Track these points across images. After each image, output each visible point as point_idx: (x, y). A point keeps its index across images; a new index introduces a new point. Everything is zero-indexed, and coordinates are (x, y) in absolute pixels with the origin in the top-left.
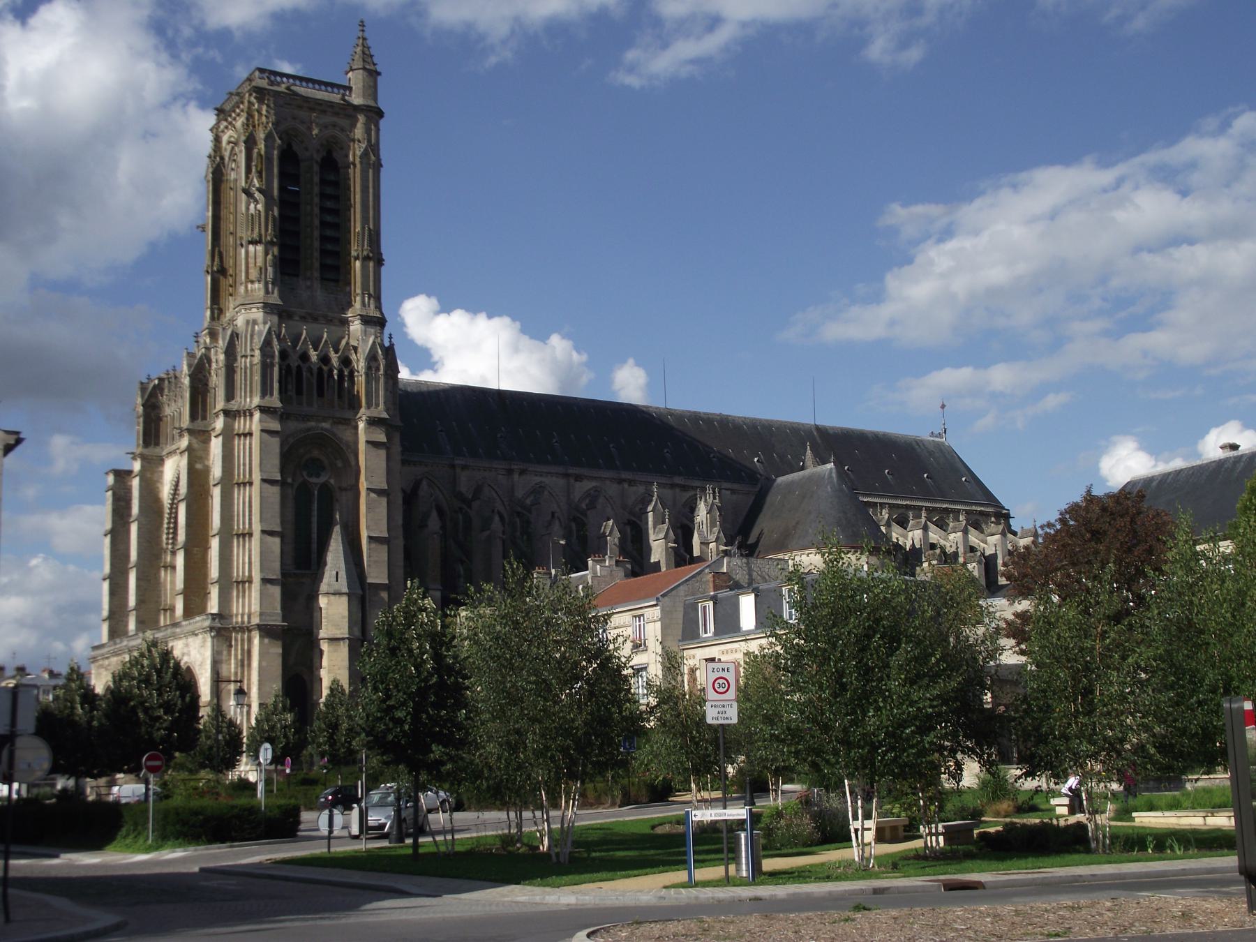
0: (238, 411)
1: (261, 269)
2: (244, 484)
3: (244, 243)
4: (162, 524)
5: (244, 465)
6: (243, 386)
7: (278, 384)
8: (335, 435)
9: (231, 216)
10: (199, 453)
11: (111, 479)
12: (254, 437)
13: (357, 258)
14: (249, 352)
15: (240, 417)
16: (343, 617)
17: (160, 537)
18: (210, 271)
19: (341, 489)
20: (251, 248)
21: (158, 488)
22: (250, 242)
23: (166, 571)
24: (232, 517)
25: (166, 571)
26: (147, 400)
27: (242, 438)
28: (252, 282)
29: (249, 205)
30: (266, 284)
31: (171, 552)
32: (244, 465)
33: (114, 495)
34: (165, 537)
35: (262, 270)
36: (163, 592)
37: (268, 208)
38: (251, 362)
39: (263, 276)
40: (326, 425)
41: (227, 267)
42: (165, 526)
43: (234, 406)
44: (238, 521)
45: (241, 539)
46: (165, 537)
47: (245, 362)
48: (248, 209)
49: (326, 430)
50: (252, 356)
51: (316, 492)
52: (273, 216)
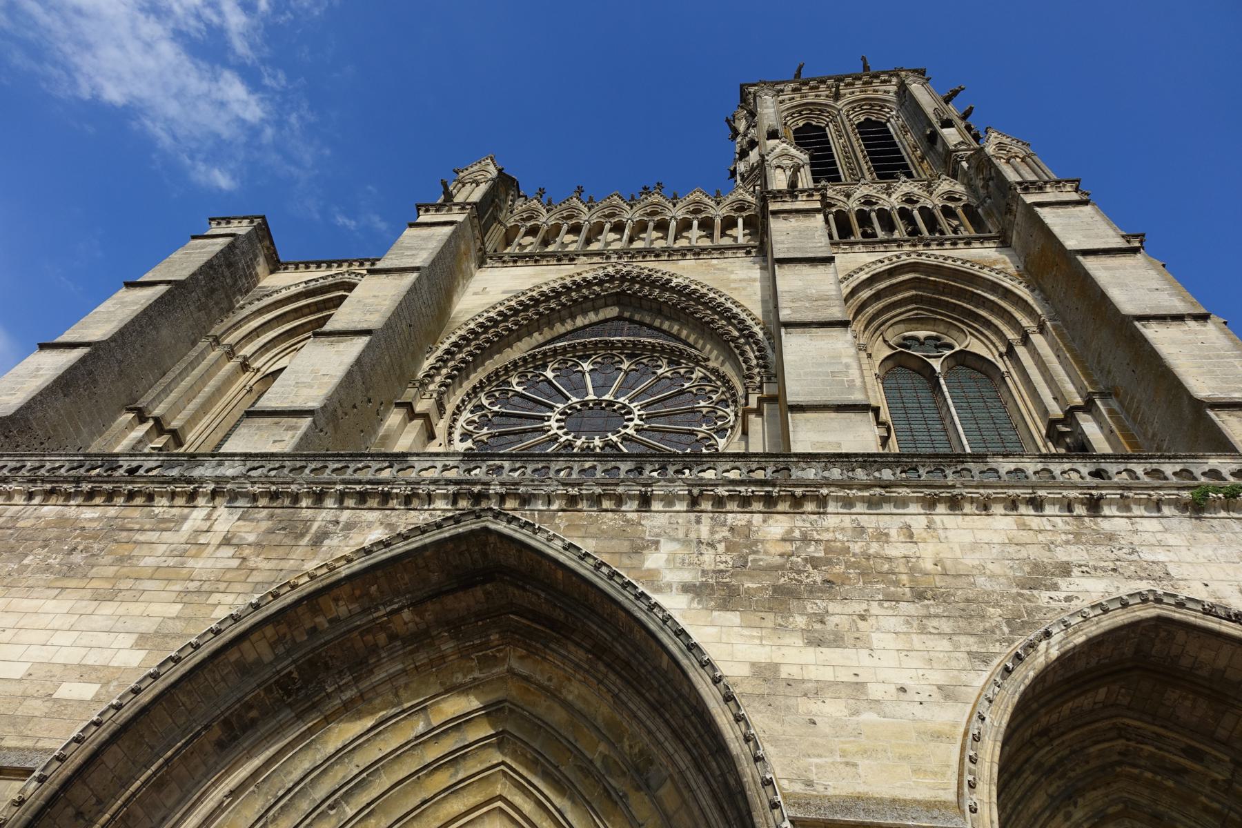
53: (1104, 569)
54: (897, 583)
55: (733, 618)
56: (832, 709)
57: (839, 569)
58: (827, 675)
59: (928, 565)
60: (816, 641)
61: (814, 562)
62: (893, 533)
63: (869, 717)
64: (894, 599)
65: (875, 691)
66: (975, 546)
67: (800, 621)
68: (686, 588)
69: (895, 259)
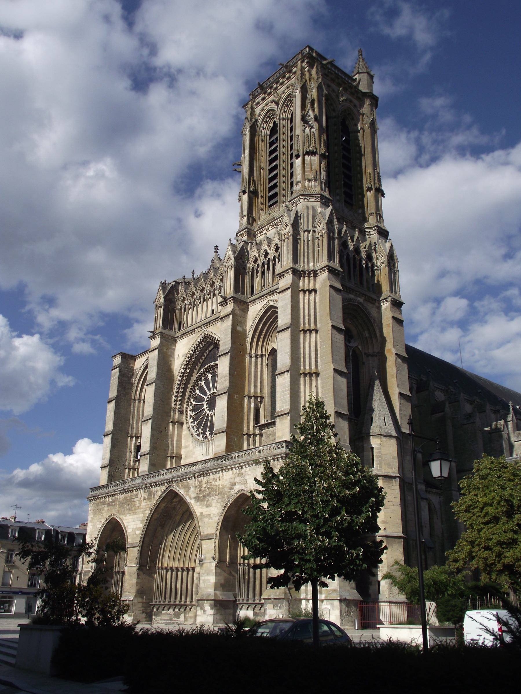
0: (304, 272)
1: (317, 172)
2: (310, 331)
3: (301, 154)
4: (172, 389)
5: (309, 315)
6: (306, 254)
7: (338, 255)
8: (366, 309)
9: (262, 158)
10: (240, 319)
11: (118, 360)
12: (318, 294)
13: (369, 189)
14: (310, 228)
15: (304, 277)
16: (393, 458)
17: (170, 399)
18: (247, 191)
19: (367, 355)
20: (307, 158)
21: (171, 361)
22: (307, 153)
23: (174, 426)
24: (299, 359)
25: (174, 426)
26: (167, 295)
27: (307, 293)
28: (309, 181)
29: (305, 129)
30: (321, 183)
31: (179, 411)
32: (309, 315)
33: (120, 371)
34: (174, 399)
35: (318, 172)
36: (170, 443)
37: (321, 130)
38: (313, 236)
39: (318, 177)
40: (361, 300)
41: (259, 191)
42: (175, 390)
43: (300, 267)
44: (304, 362)
45: (308, 378)
46: (174, 399)
47: (308, 236)
48: (304, 131)
49: (360, 303)
50: (314, 231)
51: (351, 354)
52: (324, 140)
53: (239, 483)
54: (216, 492)
55: (198, 503)
56: (206, 520)
57: (211, 490)
58: (207, 513)
59: (221, 486)
60: (207, 507)
61: (208, 488)
62: (218, 479)
63: (210, 520)
64: (216, 495)
65: (212, 515)
66: (226, 480)
67: (206, 502)
68: (195, 498)
69: (265, 306)
